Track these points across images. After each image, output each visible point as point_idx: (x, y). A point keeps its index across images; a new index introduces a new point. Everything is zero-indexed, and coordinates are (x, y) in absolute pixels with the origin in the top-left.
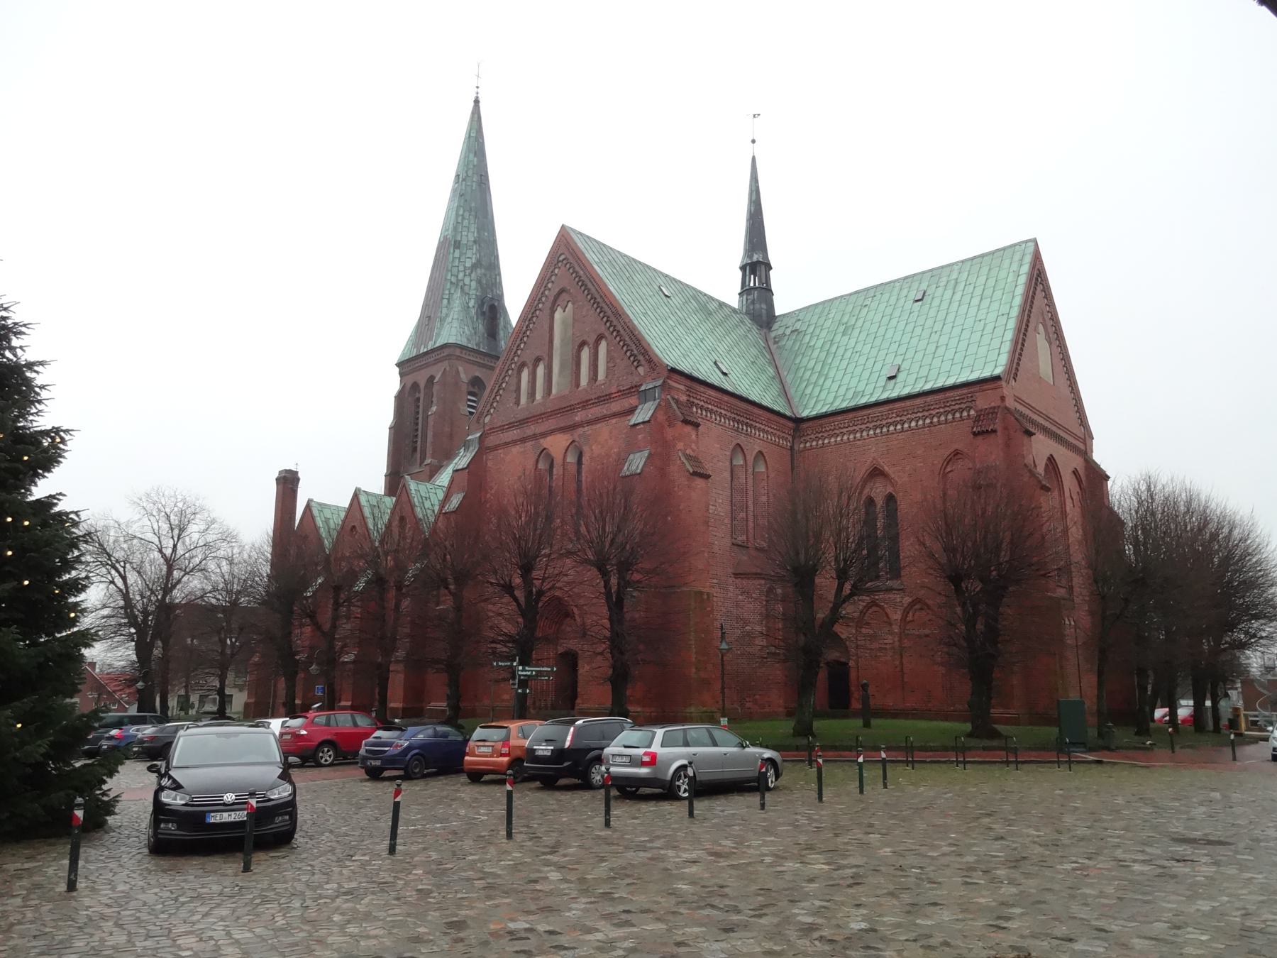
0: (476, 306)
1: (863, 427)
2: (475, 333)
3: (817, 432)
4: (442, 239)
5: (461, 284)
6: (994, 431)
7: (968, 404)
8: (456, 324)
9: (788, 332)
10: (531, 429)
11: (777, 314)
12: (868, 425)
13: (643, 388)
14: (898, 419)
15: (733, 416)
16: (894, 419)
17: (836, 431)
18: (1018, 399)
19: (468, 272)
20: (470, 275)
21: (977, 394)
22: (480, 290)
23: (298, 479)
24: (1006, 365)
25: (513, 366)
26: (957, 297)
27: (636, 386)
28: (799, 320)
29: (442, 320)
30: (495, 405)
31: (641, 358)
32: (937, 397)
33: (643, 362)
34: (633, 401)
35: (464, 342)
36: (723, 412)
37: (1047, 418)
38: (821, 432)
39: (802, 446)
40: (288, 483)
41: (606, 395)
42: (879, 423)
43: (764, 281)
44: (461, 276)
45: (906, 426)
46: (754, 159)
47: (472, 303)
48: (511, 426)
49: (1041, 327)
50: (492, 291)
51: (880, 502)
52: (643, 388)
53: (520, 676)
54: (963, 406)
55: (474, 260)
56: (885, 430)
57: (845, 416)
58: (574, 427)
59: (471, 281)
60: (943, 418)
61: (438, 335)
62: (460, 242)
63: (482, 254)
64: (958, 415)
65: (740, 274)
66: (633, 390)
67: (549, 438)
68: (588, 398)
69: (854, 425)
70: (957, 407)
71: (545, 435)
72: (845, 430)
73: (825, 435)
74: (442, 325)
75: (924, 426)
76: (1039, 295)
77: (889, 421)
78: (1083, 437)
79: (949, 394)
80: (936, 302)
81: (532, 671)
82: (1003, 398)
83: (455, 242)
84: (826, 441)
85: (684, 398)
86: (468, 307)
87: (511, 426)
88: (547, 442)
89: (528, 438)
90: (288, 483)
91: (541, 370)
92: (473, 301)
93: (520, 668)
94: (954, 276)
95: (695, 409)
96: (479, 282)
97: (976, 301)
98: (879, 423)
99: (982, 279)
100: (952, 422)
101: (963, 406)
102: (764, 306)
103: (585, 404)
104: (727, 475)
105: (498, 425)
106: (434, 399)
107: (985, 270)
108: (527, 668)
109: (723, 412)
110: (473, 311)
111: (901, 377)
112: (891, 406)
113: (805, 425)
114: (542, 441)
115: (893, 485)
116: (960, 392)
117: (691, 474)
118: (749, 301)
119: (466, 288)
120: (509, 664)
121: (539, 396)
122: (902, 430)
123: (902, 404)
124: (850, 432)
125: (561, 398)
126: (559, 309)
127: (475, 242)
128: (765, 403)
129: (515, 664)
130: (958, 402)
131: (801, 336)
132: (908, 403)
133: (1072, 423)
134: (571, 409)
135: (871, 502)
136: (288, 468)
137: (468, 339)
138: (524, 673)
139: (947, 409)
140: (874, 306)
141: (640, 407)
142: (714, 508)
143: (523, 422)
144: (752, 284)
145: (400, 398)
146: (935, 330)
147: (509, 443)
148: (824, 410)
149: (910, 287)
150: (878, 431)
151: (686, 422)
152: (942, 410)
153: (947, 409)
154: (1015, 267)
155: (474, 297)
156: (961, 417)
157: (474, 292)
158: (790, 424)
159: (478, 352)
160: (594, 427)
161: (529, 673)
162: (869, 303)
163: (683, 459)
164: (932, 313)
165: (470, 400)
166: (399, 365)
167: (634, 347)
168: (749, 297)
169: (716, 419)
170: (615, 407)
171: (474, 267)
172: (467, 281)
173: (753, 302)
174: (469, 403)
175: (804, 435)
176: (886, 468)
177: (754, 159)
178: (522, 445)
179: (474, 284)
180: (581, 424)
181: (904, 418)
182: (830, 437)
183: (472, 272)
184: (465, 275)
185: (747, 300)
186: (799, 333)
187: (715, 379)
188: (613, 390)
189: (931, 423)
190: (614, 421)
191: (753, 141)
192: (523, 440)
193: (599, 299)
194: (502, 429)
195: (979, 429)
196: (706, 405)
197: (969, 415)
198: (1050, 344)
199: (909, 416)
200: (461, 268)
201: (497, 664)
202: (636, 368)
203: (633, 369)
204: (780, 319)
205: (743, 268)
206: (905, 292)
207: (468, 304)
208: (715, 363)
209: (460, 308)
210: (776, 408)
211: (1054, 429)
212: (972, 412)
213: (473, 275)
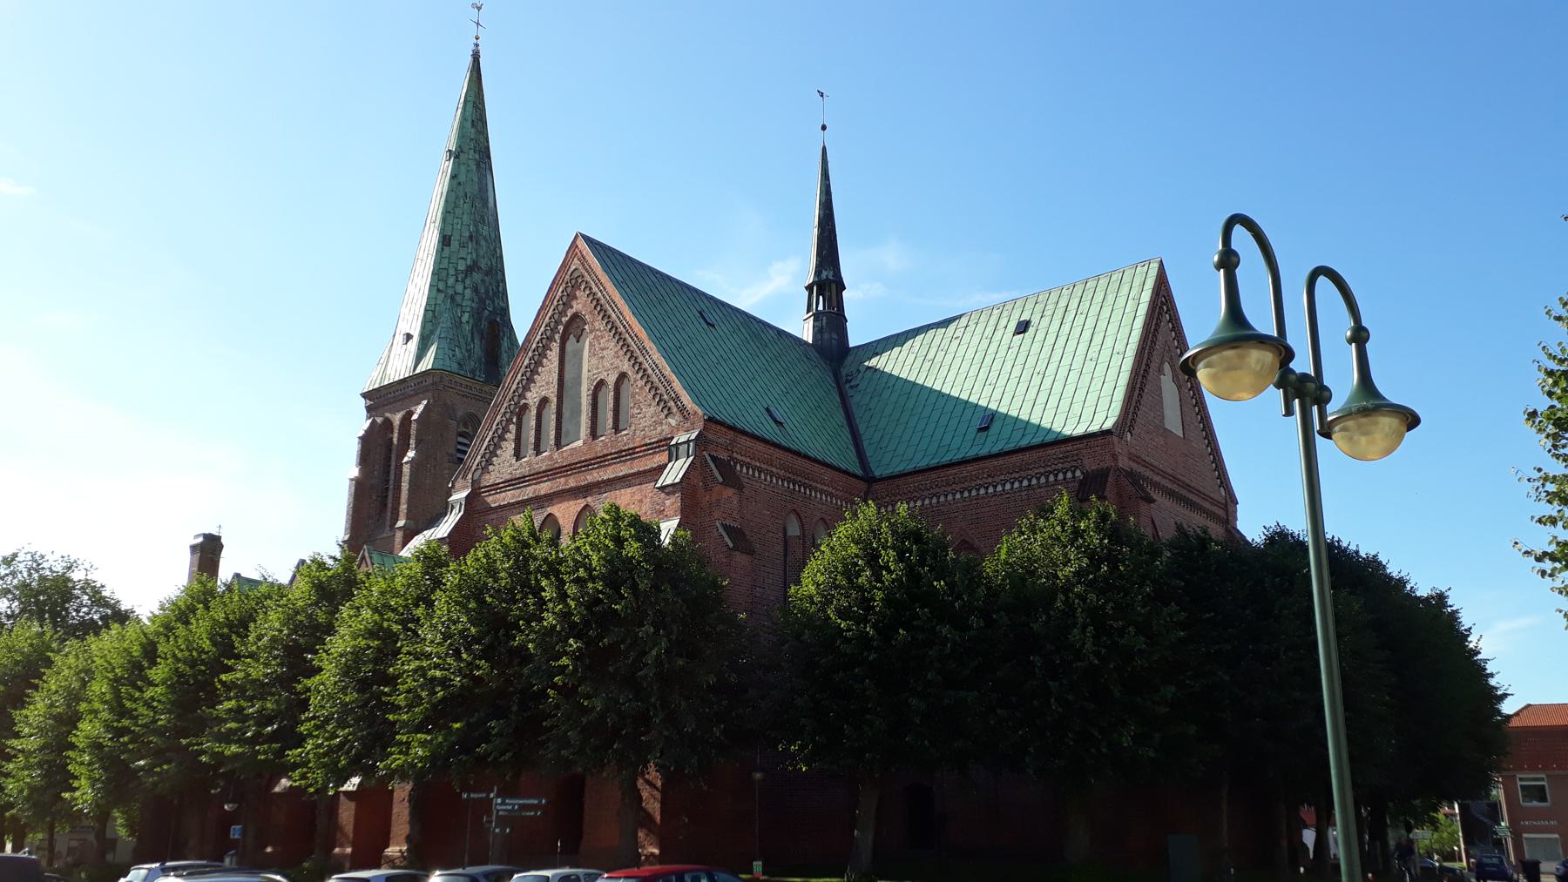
0: (471, 321)
2: (469, 357)
5: (451, 292)
11: (851, 346)
13: (673, 442)
14: (990, 480)
15: (788, 475)
17: (915, 494)
18: (1134, 458)
20: (463, 281)
22: (476, 300)
23: (222, 546)
24: (1119, 416)
27: (666, 439)
31: (672, 404)
32: (1035, 454)
33: (675, 410)
34: (663, 457)
36: (774, 470)
37: (1174, 479)
40: (208, 551)
42: (966, 484)
43: (835, 303)
44: (451, 281)
46: (824, 149)
47: (466, 317)
49: (1167, 367)
52: (673, 442)
53: (498, 811)
55: (469, 262)
59: (465, 288)
62: (450, 237)
63: (482, 253)
68: (605, 452)
71: (551, 498)
72: (926, 493)
76: (1165, 326)
78: (1223, 501)
79: (1050, 451)
80: (1040, 336)
81: (514, 805)
82: (1114, 457)
85: (724, 456)
86: (461, 322)
90: (208, 551)
92: (467, 315)
93: (499, 801)
95: (738, 468)
96: (476, 290)
98: (966, 484)
101: (1066, 465)
104: (779, 549)
106: (412, 442)
108: (507, 801)
109: (774, 470)
112: (981, 464)
113: (876, 487)
119: (458, 298)
120: (484, 795)
126: (572, 336)
127: (471, 237)
128: (828, 460)
129: (492, 795)
133: (1209, 485)
136: (207, 532)
137: (459, 364)
138: (504, 807)
141: (670, 465)
142: (762, 590)
144: (821, 308)
145: (367, 441)
148: (901, 468)
151: (726, 483)
152: (1042, 470)
153: (1049, 469)
155: (468, 309)
156: (1065, 479)
157: (469, 303)
158: (863, 486)
161: (510, 807)
163: (721, 530)
165: (460, 443)
166: (365, 395)
167: (662, 390)
169: (765, 480)
171: (470, 269)
172: (459, 288)
174: (459, 447)
176: (976, 542)
177: (824, 149)
179: (468, 292)
181: (997, 479)
183: (466, 276)
184: (457, 281)
187: (768, 430)
189: (1029, 485)
191: (824, 128)
193: (622, 329)
196: (753, 463)
197: (1074, 477)
198: (1179, 388)
199: (1002, 477)
200: (452, 272)
201: (469, 796)
205: (809, 288)
207: (460, 318)
208: (768, 410)
209: (449, 324)
210: (843, 466)
211: (1184, 492)
212: (1078, 473)
213: (468, 282)
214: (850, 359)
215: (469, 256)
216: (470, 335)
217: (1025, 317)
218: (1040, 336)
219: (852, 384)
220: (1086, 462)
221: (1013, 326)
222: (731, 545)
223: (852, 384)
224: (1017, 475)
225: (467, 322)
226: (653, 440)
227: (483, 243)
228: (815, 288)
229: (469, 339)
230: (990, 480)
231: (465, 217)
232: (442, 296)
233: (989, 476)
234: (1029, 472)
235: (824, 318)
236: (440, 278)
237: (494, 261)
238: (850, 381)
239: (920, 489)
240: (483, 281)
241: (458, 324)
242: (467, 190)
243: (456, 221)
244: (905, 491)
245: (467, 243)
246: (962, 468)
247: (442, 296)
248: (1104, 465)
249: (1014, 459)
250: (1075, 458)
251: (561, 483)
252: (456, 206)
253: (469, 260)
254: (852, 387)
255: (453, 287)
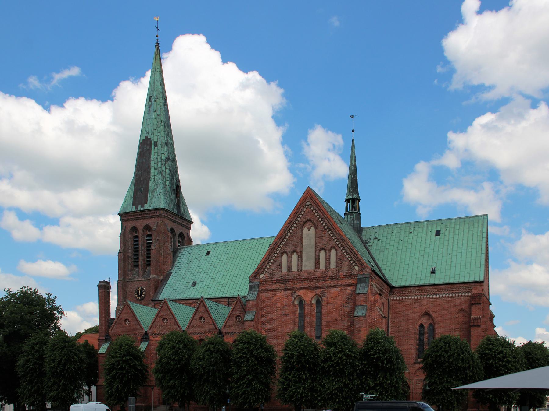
0: (170, 185)
1: (422, 294)
3: (400, 294)
4: (144, 138)
5: (160, 170)
6: (480, 304)
7: (469, 291)
8: (162, 196)
9: (372, 238)
10: (290, 285)
12: (424, 293)
13: (359, 277)
14: (438, 293)
16: (436, 292)
19: (163, 163)
20: (165, 165)
21: (473, 287)
23: (111, 287)
25: (278, 252)
26: (456, 237)
28: (376, 232)
29: (153, 192)
30: (266, 269)
31: (357, 262)
32: (456, 286)
34: (352, 281)
35: (167, 208)
38: (402, 293)
39: (392, 299)
41: (337, 276)
42: (429, 293)
44: (160, 164)
45: (441, 296)
47: (167, 183)
48: (278, 281)
50: (175, 175)
51: (426, 326)
54: (466, 291)
55: (166, 156)
56: (431, 296)
57: (414, 288)
58: (317, 288)
59: (166, 169)
60: (457, 295)
61: (151, 201)
62: (157, 142)
64: (463, 294)
65: (346, 203)
66: (351, 276)
67: (301, 291)
69: (418, 292)
70: (464, 291)
72: (413, 294)
73: (404, 295)
74: (153, 196)
75: (449, 297)
77: (434, 293)
79: (461, 285)
80: (447, 239)
83: (154, 142)
84: (404, 298)
86: (166, 185)
87: (278, 281)
88: (300, 293)
89: (289, 289)
91: (295, 257)
92: (168, 182)
94: (453, 226)
97: (465, 242)
98: (429, 293)
99: (466, 231)
100: (460, 297)
101: (466, 291)
102: (358, 222)
103: (324, 278)
105: (269, 280)
107: (467, 226)
110: (169, 188)
111: (437, 272)
112: (435, 287)
113: (394, 290)
114: (297, 292)
115: (433, 320)
116: (466, 285)
117: (383, 317)
118: (351, 219)
119: (164, 174)
121: (294, 269)
122: (439, 298)
123: (441, 287)
124: (416, 295)
125: (309, 272)
127: (166, 143)
130: (465, 289)
131: (380, 242)
132: (443, 286)
134: (315, 279)
135: (422, 326)
139: (460, 291)
140: (416, 233)
143: (285, 281)
146: (449, 253)
147: (277, 290)
149: (432, 227)
150: (428, 296)
152: (457, 291)
153: (460, 291)
154: (480, 228)
155: (168, 179)
157: (168, 176)
159: (173, 213)
160: (329, 289)
162: (412, 231)
164: (446, 243)
168: (351, 216)
170: (342, 282)
171: (167, 159)
172: (164, 169)
173: (353, 219)
175: (393, 294)
176: (431, 313)
178: (285, 292)
179: (167, 171)
180: (322, 287)
181: (440, 293)
182: (408, 296)
184: (162, 165)
185: (350, 218)
186: (378, 240)
188: (341, 274)
190: (340, 288)
192: (286, 290)
194: (272, 282)
195: (475, 302)
199: (443, 292)
200: (160, 160)
202: (354, 266)
203: (352, 266)
204: (366, 229)
206: (430, 229)
207: (165, 183)
213: (167, 165)
214: (364, 233)
215: (166, 153)
216: (170, 192)
217: (438, 229)
218: (447, 239)
219: (370, 244)
220: (473, 291)
221: (434, 232)
222: (383, 316)
223: (370, 244)
224: (448, 292)
225: (169, 185)
226: (347, 274)
227: (170, 146)
228: (351, 201)
229: (170, 193)
230: (438, 293)
231: (162, 132)
232: (156, 171)
233: (438, 291)
234: (453, 292)
235: (355, 215)
236: (155, 163)
237: (174, 155)
238: (368, 243)
239: (411, 293)
240: (172, 165)
241: (165, 186)
242: (161, 119)
243: (158, 134)
244: (405, 293)
245: (165, 146)
246: (429, 287)
247: (156, 171)
248: (479, 292)
249: (448, 286)
250: (470, 289)
251: (304, 284)
252: (158, 127)
253: (166, 155)
254: (369, 246)
255: (161, 168)
